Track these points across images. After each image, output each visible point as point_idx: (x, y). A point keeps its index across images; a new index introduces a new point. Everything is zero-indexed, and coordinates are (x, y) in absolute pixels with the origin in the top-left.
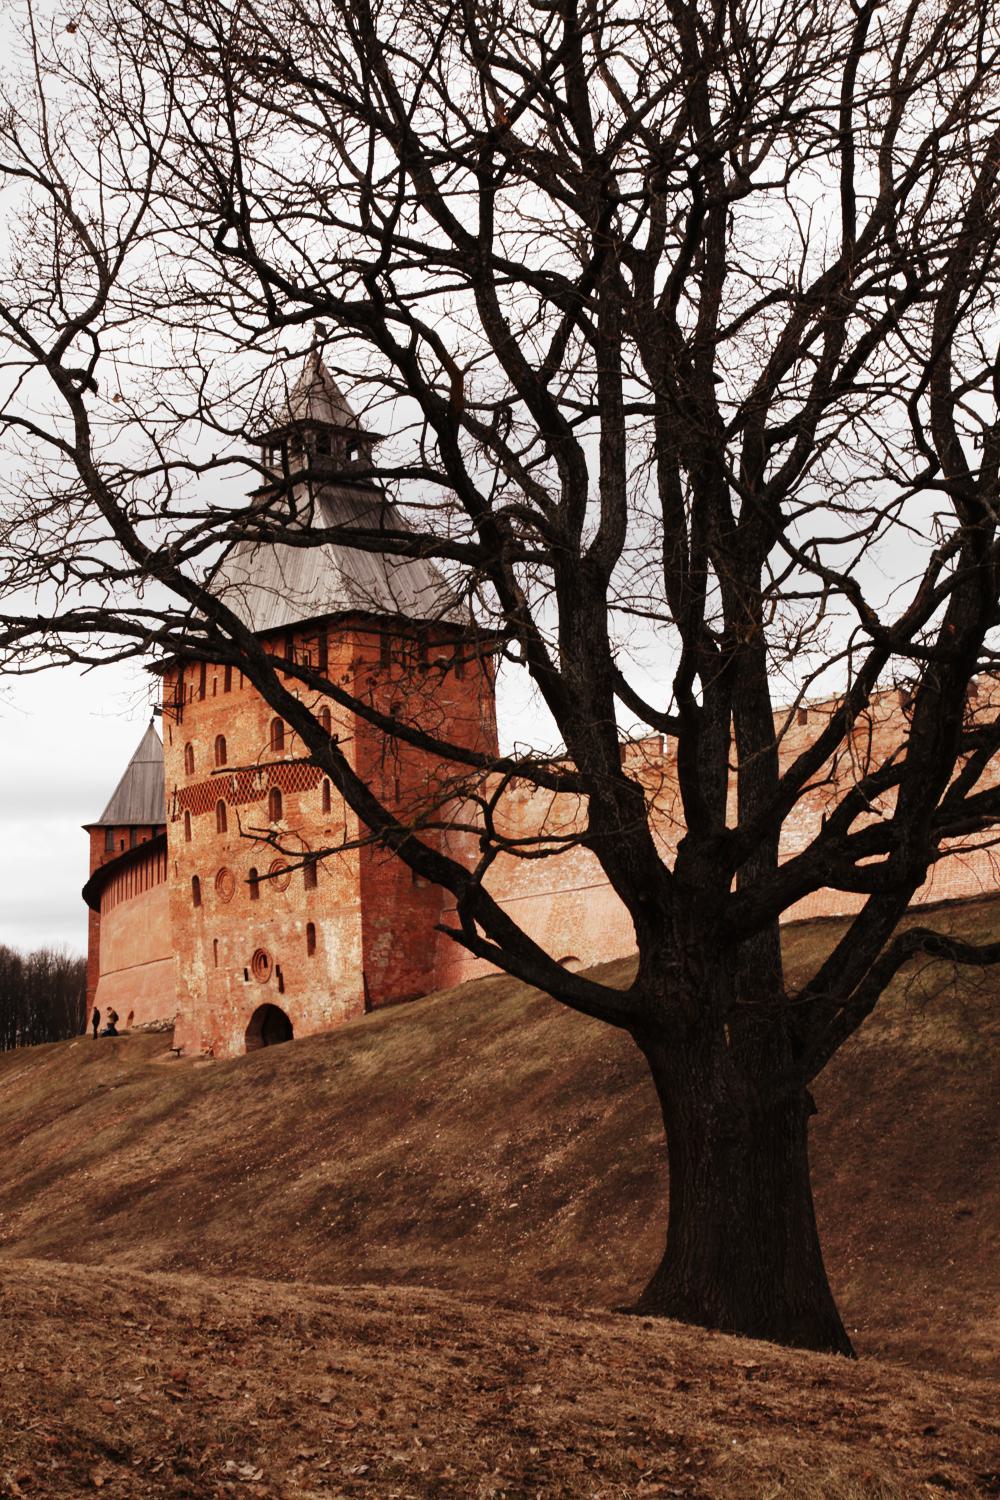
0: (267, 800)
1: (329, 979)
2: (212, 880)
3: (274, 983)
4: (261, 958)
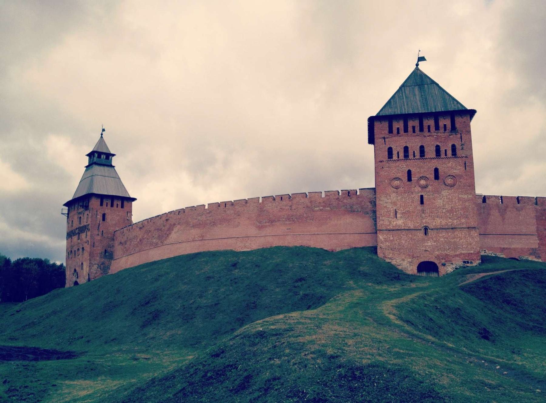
4: (75, 270)
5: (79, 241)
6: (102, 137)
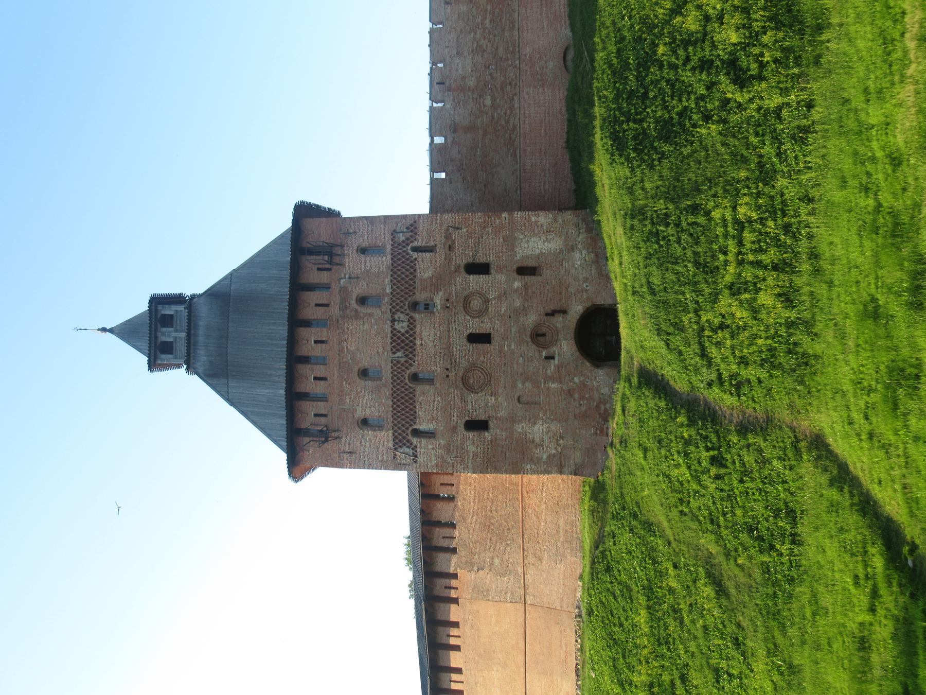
0: (416, 316)
1: (561, 251)
2: (471, 397)
3: (558, 320)
4: (538, 336)
5: (438, 300)
6: (111, 331)
